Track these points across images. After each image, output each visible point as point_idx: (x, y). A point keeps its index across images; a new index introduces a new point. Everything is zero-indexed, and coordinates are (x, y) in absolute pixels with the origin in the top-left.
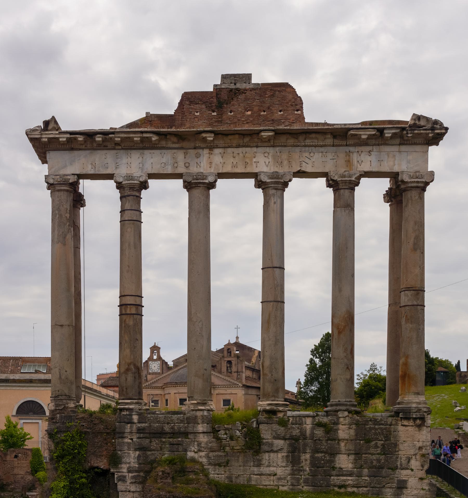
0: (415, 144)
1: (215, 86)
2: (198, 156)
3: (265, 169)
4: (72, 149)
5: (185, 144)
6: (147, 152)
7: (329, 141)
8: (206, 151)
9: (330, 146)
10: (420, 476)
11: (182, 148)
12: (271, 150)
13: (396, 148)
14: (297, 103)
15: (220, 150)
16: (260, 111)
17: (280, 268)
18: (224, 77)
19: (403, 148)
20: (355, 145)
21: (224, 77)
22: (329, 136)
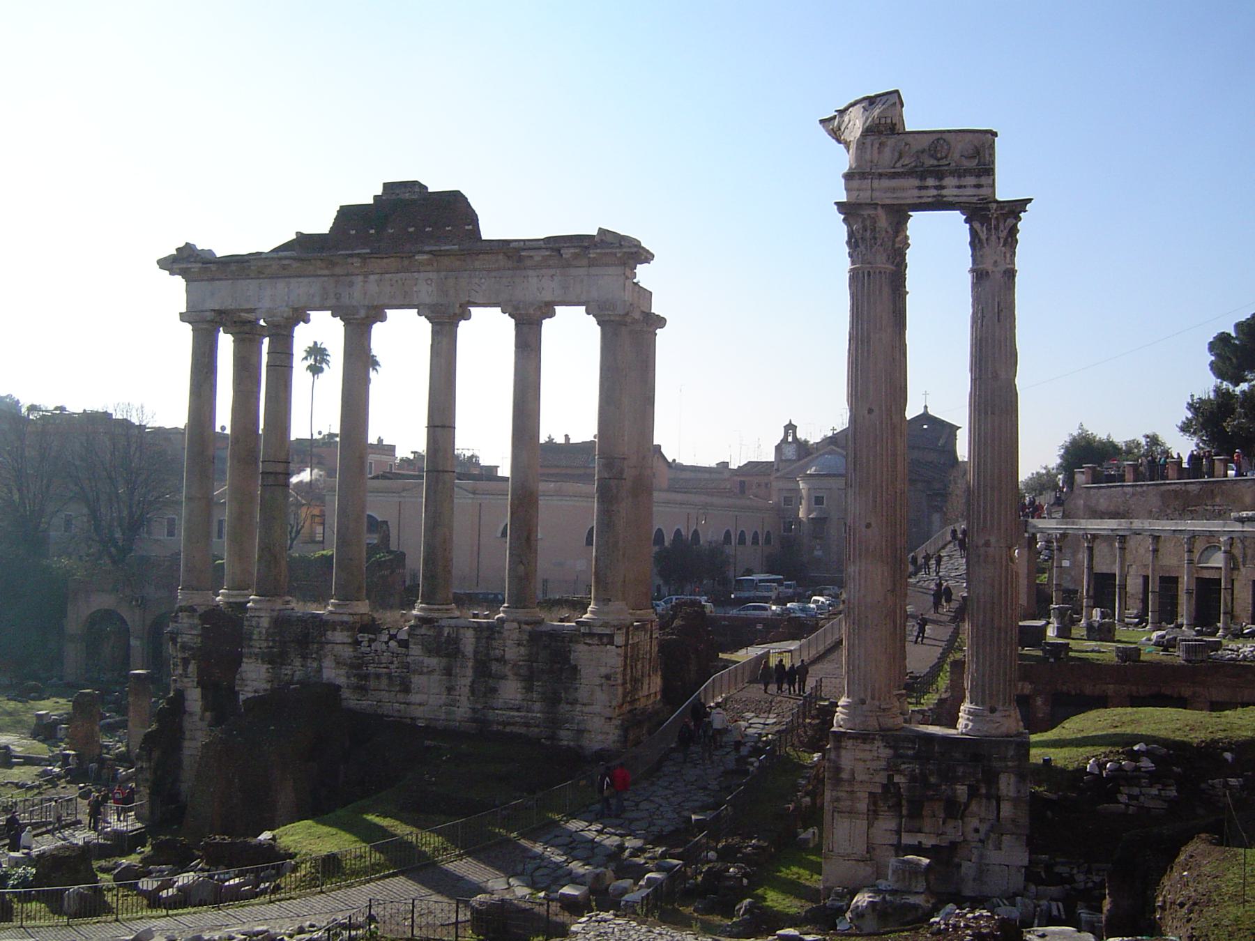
0: (607, 265)
1: (376, 197)
2: (351, 284)
3: (428, 300)
4: (213, 279)
5: (338, 270)
6: (292, 280)
7: (502, 261)
8: (361, 278)
9: (504, 269)
10: (609, 715)
11: (332, 275)
12: (433, 276)
13: (582, 271)
14: (471, 218)
15: (376, 277)
16: (425, 227)
17: (443, 427)
18: (387, 186)
19: (593, 271)
20: (534, 268)
21: (387, 186)
22: (501, 256)
